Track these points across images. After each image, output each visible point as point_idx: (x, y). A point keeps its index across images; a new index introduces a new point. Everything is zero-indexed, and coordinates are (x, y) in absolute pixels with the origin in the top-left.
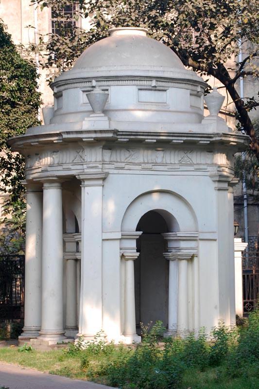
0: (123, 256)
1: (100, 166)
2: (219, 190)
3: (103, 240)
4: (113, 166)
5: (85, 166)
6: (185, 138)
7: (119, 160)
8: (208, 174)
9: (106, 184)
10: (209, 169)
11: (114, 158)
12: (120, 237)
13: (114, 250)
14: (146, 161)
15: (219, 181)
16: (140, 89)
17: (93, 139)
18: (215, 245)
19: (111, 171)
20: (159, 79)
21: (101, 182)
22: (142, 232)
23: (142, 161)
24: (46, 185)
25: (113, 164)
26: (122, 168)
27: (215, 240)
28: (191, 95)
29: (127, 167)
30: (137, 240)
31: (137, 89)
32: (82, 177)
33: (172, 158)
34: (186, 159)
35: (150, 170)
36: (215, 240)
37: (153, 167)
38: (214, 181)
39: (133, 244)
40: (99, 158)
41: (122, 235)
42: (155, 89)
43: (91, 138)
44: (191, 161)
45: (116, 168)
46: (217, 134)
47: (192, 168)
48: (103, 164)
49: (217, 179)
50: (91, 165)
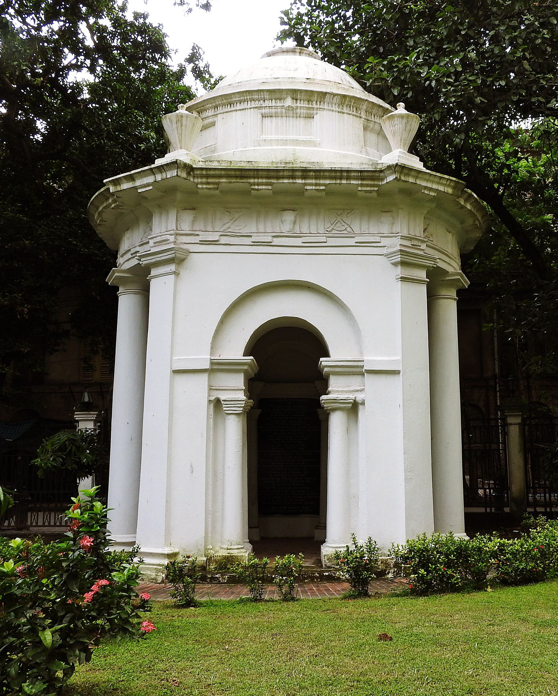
0: (217, 403)
1: (172, 238)
2: (404, 279)
3: (177, 372)
4: (197, 239)
5: (151, 242)
6: (328, 182)
7: (209, 229)
8: (384, 251)
9: (183, 273)
10: (385, 242)
11: (199, 225)
12: (207, 366)
13: (196, 391)
14: (262, 230)
15: (403, 264)
16: (264, 116)
17: (151, 188)
18: (397, 382)
19: (192, 248)
20: (295, 93)
21: (172, 267)
22: (252, 357)
23: (254, 229)
24: (121, 290)
25: (198, 235)
26: (214, 243)
27: (395, 373)
28: (365, 128)
29: (224, 240)
30: (246, 373)
31: (260, 116)
32: (145, 261)
33: (314, 227)
34: (339, 224)
35: (269, 244)
36: (395, 373)
37: (275, 239)
38: (395, 264)
39: (238, 381)
40: (172, 225)
41: (212, 363)
42: (291, 113)
43: (148, 185)
44: (349, 229)
45: (203, 243)
46: (389, 167)
47: (352, 242)
48: (177, 234)
49: (398, 258)
50: (158, 239)
